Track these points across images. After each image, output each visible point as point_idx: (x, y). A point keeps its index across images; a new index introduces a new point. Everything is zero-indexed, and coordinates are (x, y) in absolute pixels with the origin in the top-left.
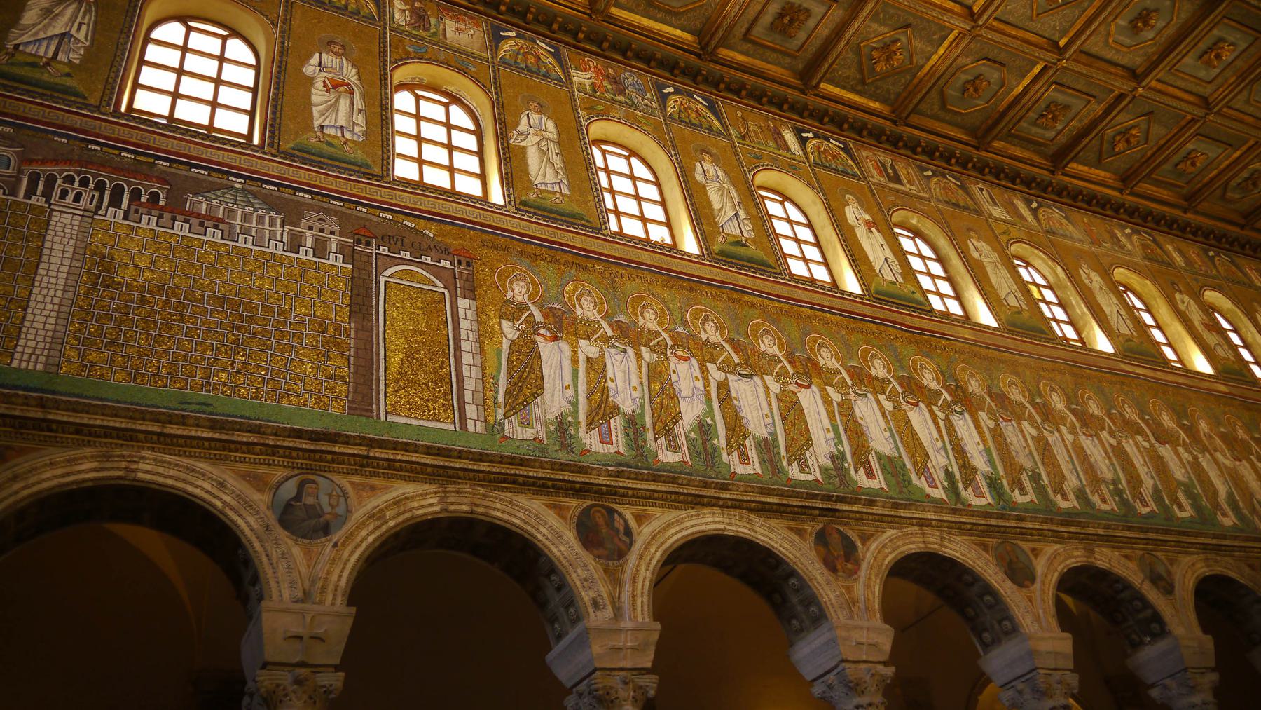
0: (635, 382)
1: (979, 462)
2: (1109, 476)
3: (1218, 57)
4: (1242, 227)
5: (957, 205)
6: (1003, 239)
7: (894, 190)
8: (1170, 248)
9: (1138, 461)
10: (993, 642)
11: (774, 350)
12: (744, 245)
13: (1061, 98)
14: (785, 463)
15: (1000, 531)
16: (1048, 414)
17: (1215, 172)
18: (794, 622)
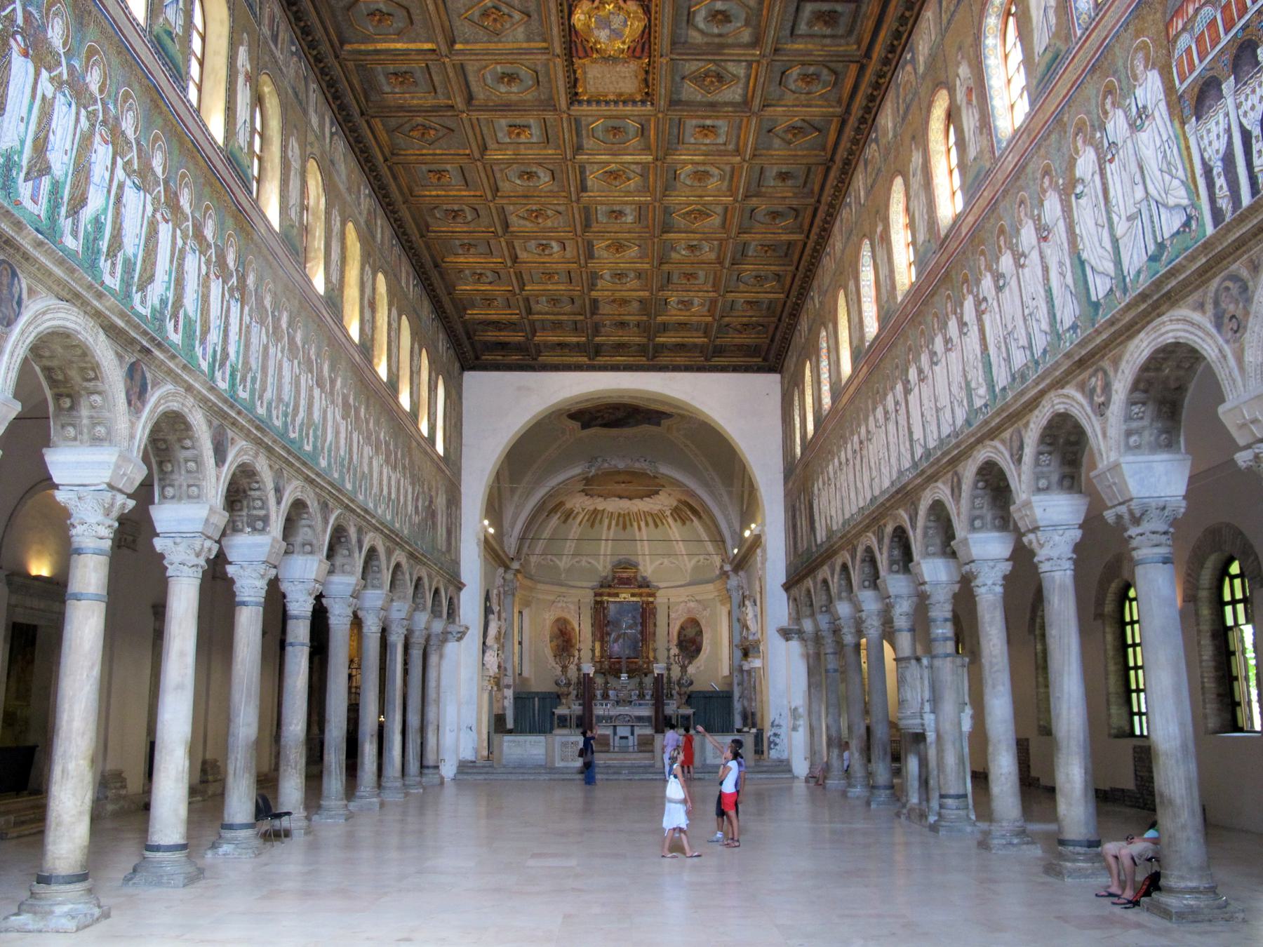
0: (68, 146)
1: (232, 350)
2: (286, 398)
3: (518, 134)
4: (422, 236)
5: (296, 94)
6: (309, 149)
7: (271, 51)
8: (379, 222)
9: (303, 395)
10: (173, 497)
11: (159, 170)
12: (173, 40)
13: (418, 74)
14: (134, 289)
15: (225, 416)
16: (277, 327)
18: (71, 429)
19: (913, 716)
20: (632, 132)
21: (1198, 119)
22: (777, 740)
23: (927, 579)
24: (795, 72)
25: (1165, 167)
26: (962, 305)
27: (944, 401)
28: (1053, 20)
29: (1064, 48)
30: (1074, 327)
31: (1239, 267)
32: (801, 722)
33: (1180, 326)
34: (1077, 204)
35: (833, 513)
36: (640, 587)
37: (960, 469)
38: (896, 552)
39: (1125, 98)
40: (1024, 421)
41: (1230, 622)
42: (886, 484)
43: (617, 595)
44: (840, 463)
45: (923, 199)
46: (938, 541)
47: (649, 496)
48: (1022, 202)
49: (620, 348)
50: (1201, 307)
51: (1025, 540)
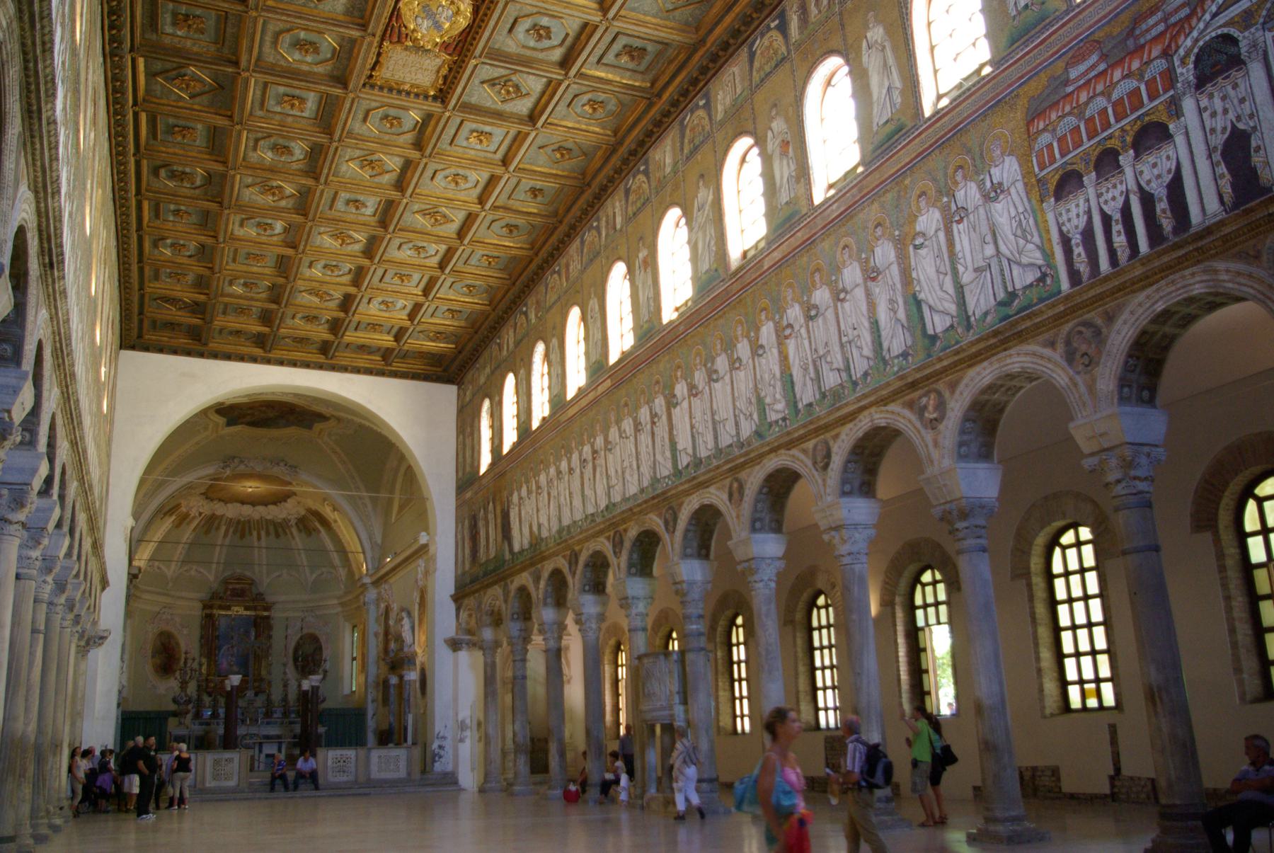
17: (181, 152)
19: (662, 708)
20: (408, 125)
21: (1058, 199)
22: (442, 753)
23: (685, 578)
24: (585, 98)
25: (1019, 232)
26: (758, 329)
27: (725, 412)
28: (898, 99)
29: (910, 124)
30: (905, 355)
31: (1095, 316)
32: (468, 733)
33: (1028, 359)
34: (915, 254)
35: (544, 520)
36: (253, 600)
37: (742, 475)
38: (635, 556)
39: (977, 173)
40: (833, 433)
41: (920, 622)
42: (633, 489)
43: (228, 608)
44: (559, 472)
45: (711, 231)
46: (695, 544)
47: (275, 503)
48: (846, 247)
49: (302, 341)
50: (1052, 344)
51: (826, 537)
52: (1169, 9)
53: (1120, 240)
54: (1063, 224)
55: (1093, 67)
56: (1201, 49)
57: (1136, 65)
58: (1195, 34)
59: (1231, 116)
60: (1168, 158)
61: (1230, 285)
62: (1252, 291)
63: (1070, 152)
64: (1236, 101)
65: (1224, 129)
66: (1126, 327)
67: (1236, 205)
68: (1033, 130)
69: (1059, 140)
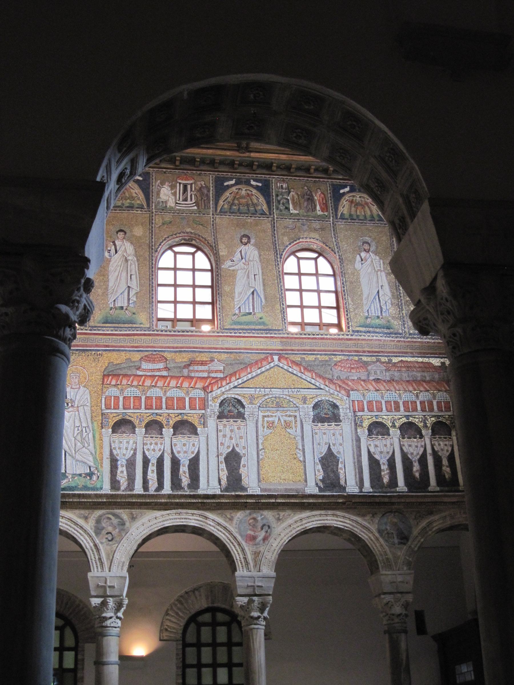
21: (113, 432)
25: (79, 438)
31: (124, 514)
50: (86, 518)
52: (212, 368)
53: (152, 475)
54: (115, 448)
55: (159, 370)
56: (224, 399)
57: (186, 384)
58: (223, 389)
59: (233, 441)
60: (194, 445)
61: (213, 528)
62: (224, 536)
63: (130, 409)
64: (238, 436)
65: (228, 447)
66: (142, 528)
67: (227, 489)
68: (108, 381)
69: (124, 398)
